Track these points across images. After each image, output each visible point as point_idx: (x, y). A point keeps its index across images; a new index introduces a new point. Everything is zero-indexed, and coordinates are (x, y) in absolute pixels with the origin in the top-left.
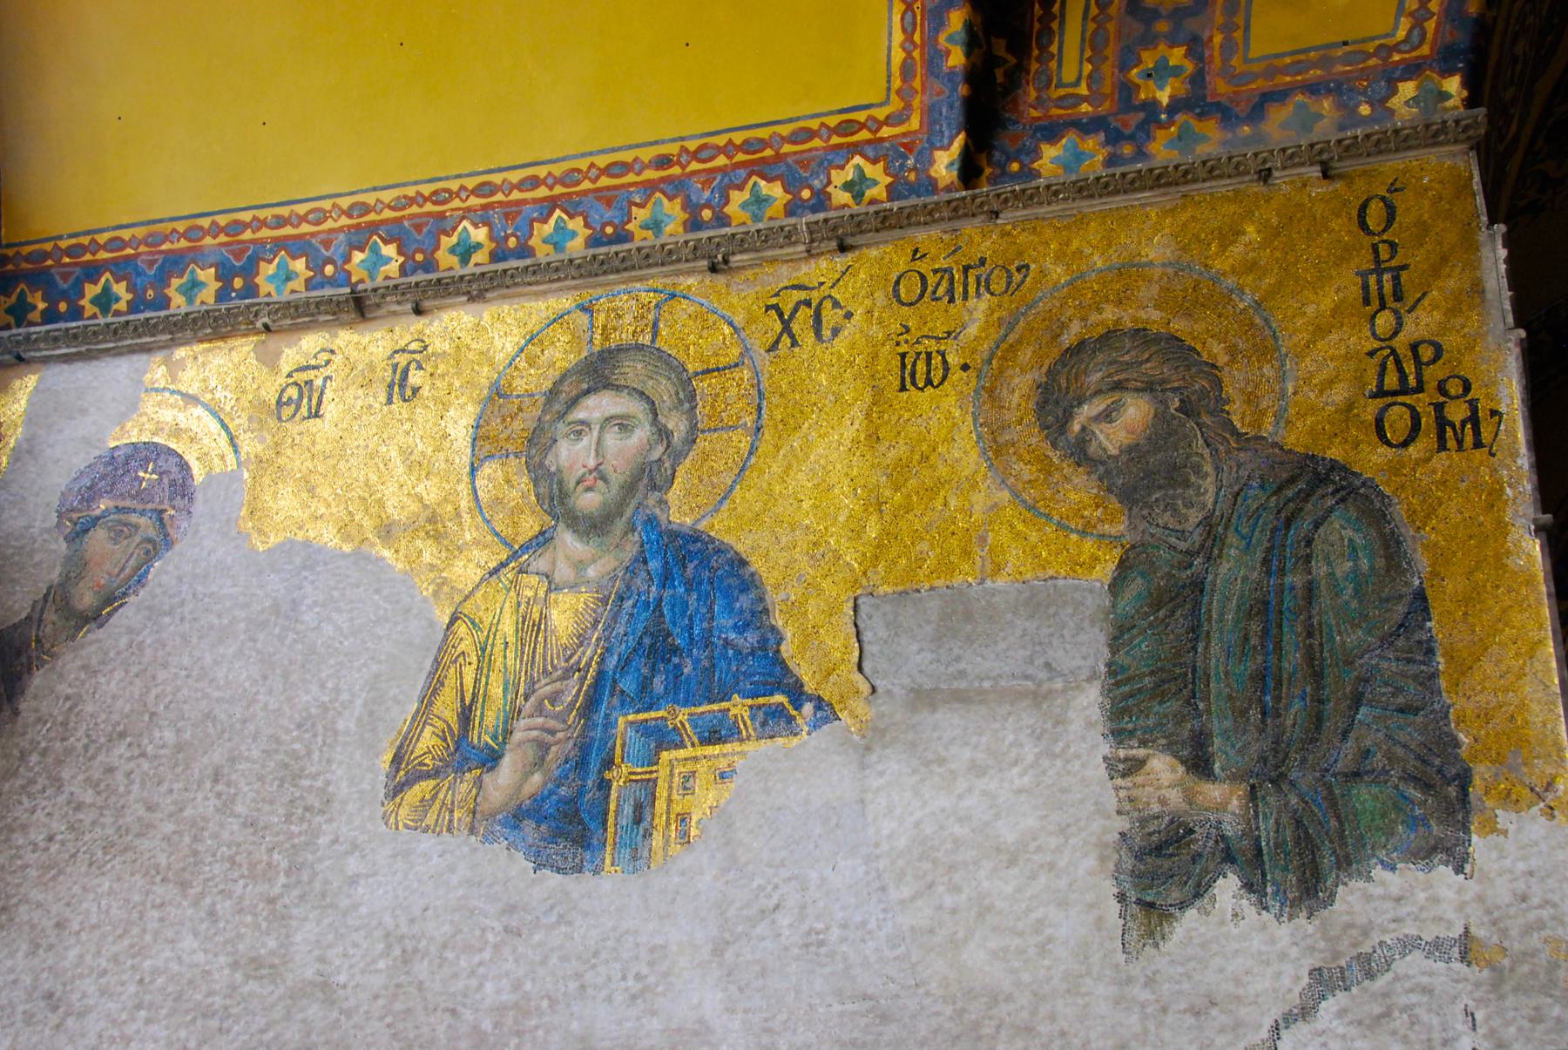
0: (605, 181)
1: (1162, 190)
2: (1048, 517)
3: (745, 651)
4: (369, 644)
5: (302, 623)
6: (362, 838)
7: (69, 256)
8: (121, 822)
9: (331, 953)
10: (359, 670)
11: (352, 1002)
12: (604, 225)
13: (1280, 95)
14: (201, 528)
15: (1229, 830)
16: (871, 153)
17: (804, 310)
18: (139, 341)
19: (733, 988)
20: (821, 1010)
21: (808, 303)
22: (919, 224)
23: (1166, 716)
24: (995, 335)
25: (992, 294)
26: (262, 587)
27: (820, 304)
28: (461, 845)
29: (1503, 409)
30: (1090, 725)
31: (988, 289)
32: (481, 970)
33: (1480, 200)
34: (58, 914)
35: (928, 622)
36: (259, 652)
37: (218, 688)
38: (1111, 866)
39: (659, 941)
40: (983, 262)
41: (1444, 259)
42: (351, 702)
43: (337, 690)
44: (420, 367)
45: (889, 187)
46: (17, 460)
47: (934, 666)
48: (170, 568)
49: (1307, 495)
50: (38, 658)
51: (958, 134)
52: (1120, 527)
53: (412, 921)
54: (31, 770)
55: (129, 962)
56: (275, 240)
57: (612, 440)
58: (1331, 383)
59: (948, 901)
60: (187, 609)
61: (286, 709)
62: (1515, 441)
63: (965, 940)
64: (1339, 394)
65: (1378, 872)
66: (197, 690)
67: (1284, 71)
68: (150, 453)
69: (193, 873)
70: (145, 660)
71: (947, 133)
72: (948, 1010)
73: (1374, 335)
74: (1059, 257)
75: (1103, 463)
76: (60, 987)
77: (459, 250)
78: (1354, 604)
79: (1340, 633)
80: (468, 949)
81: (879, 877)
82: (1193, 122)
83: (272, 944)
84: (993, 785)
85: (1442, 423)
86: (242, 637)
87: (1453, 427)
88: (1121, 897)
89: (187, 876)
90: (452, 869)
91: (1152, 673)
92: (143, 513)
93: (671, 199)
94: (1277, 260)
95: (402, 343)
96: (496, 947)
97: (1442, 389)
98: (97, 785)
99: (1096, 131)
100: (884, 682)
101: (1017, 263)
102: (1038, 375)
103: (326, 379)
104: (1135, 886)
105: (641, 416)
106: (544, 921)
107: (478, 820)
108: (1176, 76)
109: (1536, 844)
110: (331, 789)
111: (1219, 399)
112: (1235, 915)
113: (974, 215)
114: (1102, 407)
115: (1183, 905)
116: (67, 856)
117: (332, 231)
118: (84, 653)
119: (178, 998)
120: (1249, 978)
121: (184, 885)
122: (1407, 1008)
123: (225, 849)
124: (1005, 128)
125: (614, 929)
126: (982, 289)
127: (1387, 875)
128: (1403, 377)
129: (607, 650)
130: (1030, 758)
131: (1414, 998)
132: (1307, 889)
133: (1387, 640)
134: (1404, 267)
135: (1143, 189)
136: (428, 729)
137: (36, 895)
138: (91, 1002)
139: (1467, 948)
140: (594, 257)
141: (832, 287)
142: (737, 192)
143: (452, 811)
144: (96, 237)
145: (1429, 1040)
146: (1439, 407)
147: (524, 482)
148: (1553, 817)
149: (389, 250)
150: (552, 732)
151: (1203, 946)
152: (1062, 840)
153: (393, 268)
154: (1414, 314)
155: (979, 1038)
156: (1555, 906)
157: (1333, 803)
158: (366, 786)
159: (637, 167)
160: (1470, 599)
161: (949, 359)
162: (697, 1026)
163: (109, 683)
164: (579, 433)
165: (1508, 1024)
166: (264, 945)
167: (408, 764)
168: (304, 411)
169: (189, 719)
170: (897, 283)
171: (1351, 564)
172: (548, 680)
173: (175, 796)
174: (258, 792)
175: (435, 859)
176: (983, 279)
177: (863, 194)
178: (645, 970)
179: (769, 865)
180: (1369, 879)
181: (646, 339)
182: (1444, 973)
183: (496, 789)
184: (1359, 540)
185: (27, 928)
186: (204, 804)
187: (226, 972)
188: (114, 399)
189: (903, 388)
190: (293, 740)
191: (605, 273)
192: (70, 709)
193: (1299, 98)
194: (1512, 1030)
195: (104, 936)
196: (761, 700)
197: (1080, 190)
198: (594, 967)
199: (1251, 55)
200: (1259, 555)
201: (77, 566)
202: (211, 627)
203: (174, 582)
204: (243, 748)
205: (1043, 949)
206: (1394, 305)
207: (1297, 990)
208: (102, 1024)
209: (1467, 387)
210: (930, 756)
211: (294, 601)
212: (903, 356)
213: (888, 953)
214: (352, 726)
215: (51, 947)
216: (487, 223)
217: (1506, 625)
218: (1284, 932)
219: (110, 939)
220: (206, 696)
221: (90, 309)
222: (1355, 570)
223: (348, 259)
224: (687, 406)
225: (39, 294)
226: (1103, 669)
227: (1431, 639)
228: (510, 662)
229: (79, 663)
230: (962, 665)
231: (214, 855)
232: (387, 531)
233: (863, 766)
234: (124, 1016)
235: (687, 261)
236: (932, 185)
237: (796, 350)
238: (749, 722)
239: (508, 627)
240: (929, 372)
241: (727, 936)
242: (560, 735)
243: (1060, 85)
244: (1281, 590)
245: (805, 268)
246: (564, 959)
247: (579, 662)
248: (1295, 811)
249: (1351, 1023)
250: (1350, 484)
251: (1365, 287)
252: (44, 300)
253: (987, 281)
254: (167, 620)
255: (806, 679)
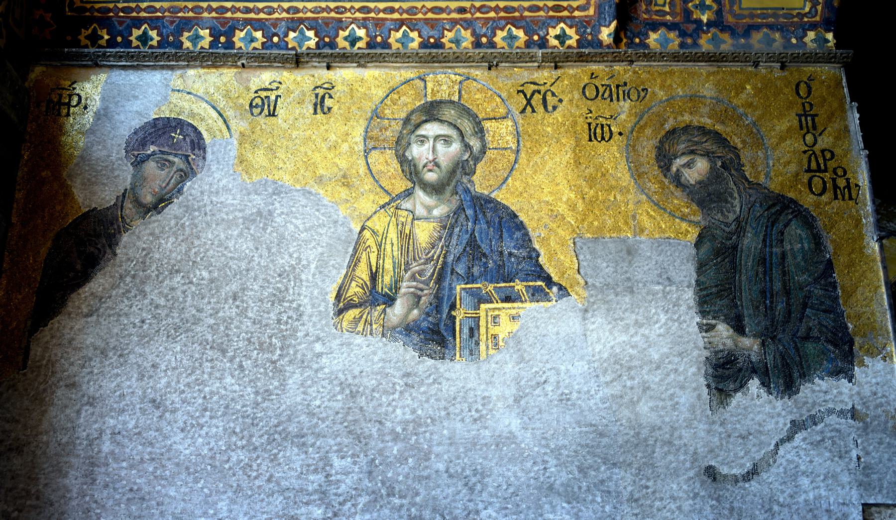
0: (430, 15)
1: (710, 63)
2: (665, 209)
3: (520, 259)
4: (316, 237)
5: (275, 222)
6: (322, 335)
7: (123, 12)
8: (182, 316)
9: (310, 390)
10: (311, 250)
11: (324, 415)
12: (429, 37)
13: (757, 27)
14: (212, 167)
15: (754, 359)
16: (569, 22)
17: (536, 96)
18: (169, 63)
19: (526, 418)
20: (570, 430)
21: (539, 92)
22: (595, 62)
23: (723, 306)
24: (634, 120)
25: (631, 100)
26: (250, 202)
27: (545, 93)
28: (377, 341)
29: (861, 184)
30: (689, 308)
31: (629, 97)
32: (394, 403)
33: (846, 90)
34: (152, 361)
35: (611, 254)
36: (252, 235)
37: (231, 252)
38: (703, 372)
39: (486, 394)
40: (625, 84)
41: (833, 114)
42: (308, 265)
43: (299, 259)
44: (331, 97)
45: (578, 41)
46: (99, 119)
47: (615, 274)
48: (196, 186)
49: (779, 212)
50: (124, 227)
51: (613, 21)
52: (698, 218)
53: (355, 377)
54: (128, 285)
55: (197, 388)
56: (245, 19)
57: (440, 147)
58: (789, 163)
59: (629, 383)
60: (208, 209)
61: (270, 265)
62: (866, 199)
63: (638, 401)
64: (793, 168)
65: (817, 380)
66: (218, 252)
67: (758, 16)
68: (179, 124)
69: (227, 346)
70: (187, 233)
71: (608, 19)
72: (632, 433)
73: (805, 143)
74: (662, 87)
75: (688, 187)
76: (159, 398)
77: (349, 39)
78: (802, 263)
79: (797, 276)
80: (386, 392)
81: (595, 371)
82: (718, 33)
83: (276, 383)
84: (647, 332)
85: (835, 187)
86: (241, 227)
87: (840, 189)
88: (708, 386)
89: (224, 346)
90: (375, 353)
91: (716, 286)
92: (176, 155)
93: (465, 29)
94: (762, 104)
95: (319, 83)
96: (401, 392)
97: (835, 171)
98: (166, 296)
99: (674, 30)
100: (591, 280)
101: (642, 87)
102: (655, 142)
103: (277, 97)
104: (714, 381)
105: (455, 137)
106: (427, 381)
107: (388, 331)
108: (710, 10)
109: (880, 372)
110: (301, 309)
111: (739, 164)
112: (758, 396)
113: (623, 61)
114: (686, 161)
115: (736, 391)
116: (154, 331)
117: (277, 19)
118: (151, 226)
119: (227, 407)
120: (765, 424)
121: (224, 352)
122: (831, 438)
123: (244, 334)
124: (632, 21)
125: (463, 387)
126: (626, 97)
127: (821, 382)
128: (818, 164)
129: (447, 252)
130: (663, 321)
131: (833, 434)
132: (788, 386)
133: (816, 280)
134: (816, 115)
135: (702, 61)
136: (354, 284)
137: (138, 350)
138: (178, 406)
139: (854, 414)
140: (430, 53)
141: (551, 86)
142: (500, 31)
143: (371, 325)
144: (139, 4)
145: (840, 451)
146: (834, 180)
147: (395, 164)
148: (885, 361)
149: (310, 34)
150: (422, 290)
151: (745, 408)
152: (680, 359)
153: (312, 43)
154: (821, 137)
155: (647, 446)
156: (887, 397)
157: (797, 349)
158: (322, 309)
159: (448, 10)
160: (851, 265)
161: (612, 129)
162: (508, 435)
163: (167, 244)
164: (422, 142)
165: (870, 445)
166: (271, 384)
167: (344, 300)
168: (266, 112)
169: (215, 266)
170: (584, 88)
171: (800, 245)
172: (416, 264)
173: (212, 305)
174: (260, 307)
175: (365, 348)
176: (626, 92)
177: (565, 42)
178: (480, 408)
179: (541, 362)
180: (813, 383)
181: (456, 98)
182: (845, 424)
183: (395, 316)
184: (804, 236)
185: (135, 366)
186: (229, 310)
187: (252, 396)
188: (153, 93)
189: (590, 140)
190: (277, 282)
191: (434, 62)
192: (146, 255)
193: (765, 30)
194: (872, 447)
195: (180, 374)
196: (531, 284)
197: (675, 57)
198: (454, 405)
199: (743, 6)
200: (761, 237)
201: (139, 180)
202: (223, 220)
203: (199, 194)
204: (249, 284)
205: (674, 407)
206: (813, 132)
207: (786, 429)
208: (185, 417)
209: (845, 173)
210: (616, 317)
211: (269, 210)
212: (589, 124)
213: (600, 405)
214: (310, 278)
215: (151, 377)
216: (365, 27)
217: (865, 278)
218: (779, 404)
219: (184, 375)
220: (223, 255)
221: (135, 43)
222: (803, 247)
223: (286, 35)
224: (480, 135)
225: (105, 31)
226: (694, 282)
227: (835, 282)
228: (395, 254)
229: (148, 231)
230: (628, 275)
231: (238, 337)
232: (320, 180)
233: (584, 319)
234: (197, 414)
235: (477, 62)
236: (600, 43)
237: (535, 114)
238: (525, 294)
239: (393, 235)
240: (603, 134)
241: (521, 393)
242: (426, 292)
243: (656, 5)
244: (771, 253)
245: (536, 75)
246: (438, 400)
247: (433, 256)
248: (782, 353)
249: (808, 444)
250: (799, 210)
251: (800, 121)
252: (108, 34)
253: (628, 93)
254: (197, 213)
255: (552, 275)
